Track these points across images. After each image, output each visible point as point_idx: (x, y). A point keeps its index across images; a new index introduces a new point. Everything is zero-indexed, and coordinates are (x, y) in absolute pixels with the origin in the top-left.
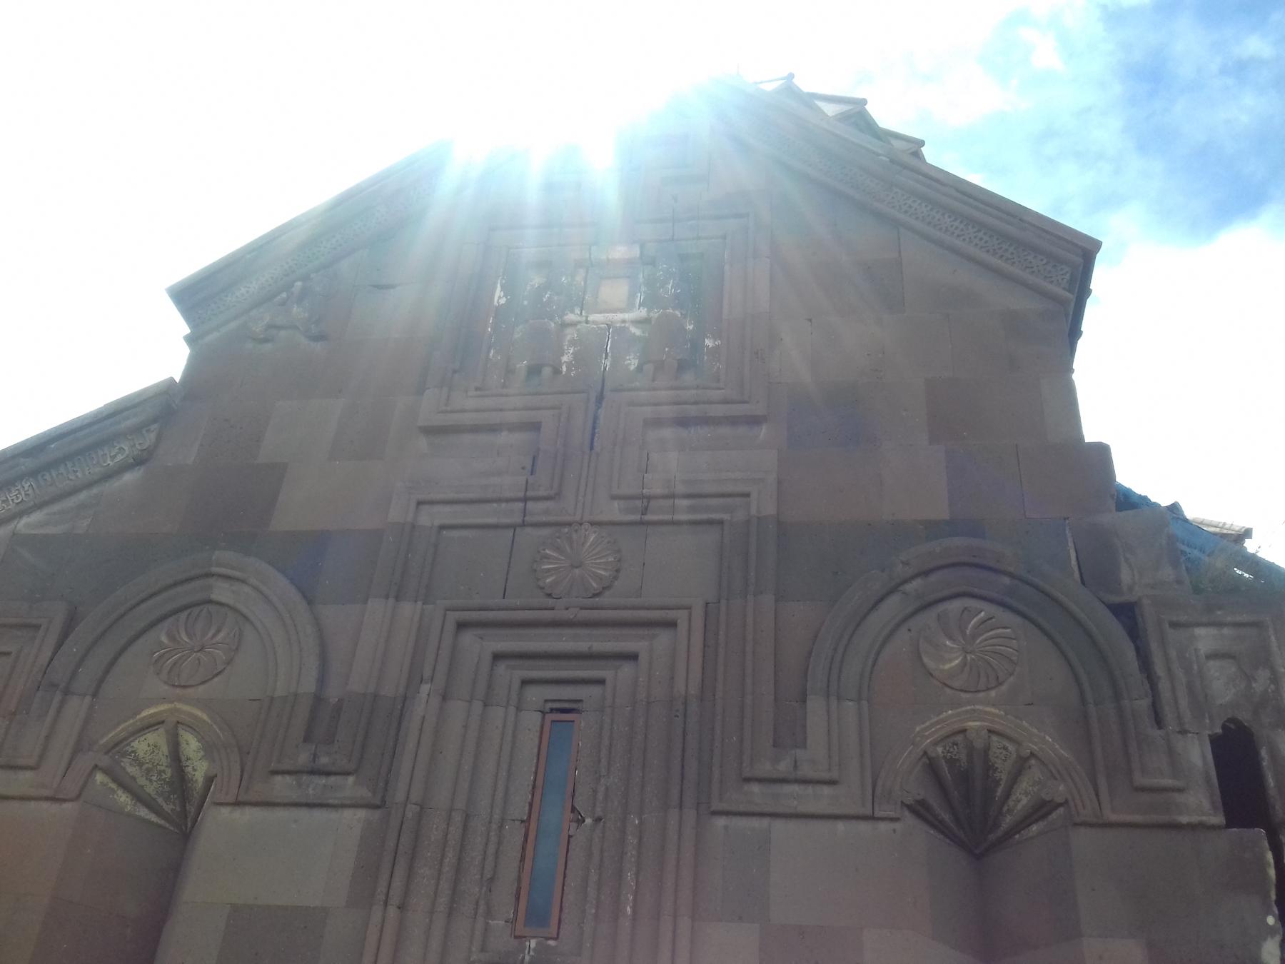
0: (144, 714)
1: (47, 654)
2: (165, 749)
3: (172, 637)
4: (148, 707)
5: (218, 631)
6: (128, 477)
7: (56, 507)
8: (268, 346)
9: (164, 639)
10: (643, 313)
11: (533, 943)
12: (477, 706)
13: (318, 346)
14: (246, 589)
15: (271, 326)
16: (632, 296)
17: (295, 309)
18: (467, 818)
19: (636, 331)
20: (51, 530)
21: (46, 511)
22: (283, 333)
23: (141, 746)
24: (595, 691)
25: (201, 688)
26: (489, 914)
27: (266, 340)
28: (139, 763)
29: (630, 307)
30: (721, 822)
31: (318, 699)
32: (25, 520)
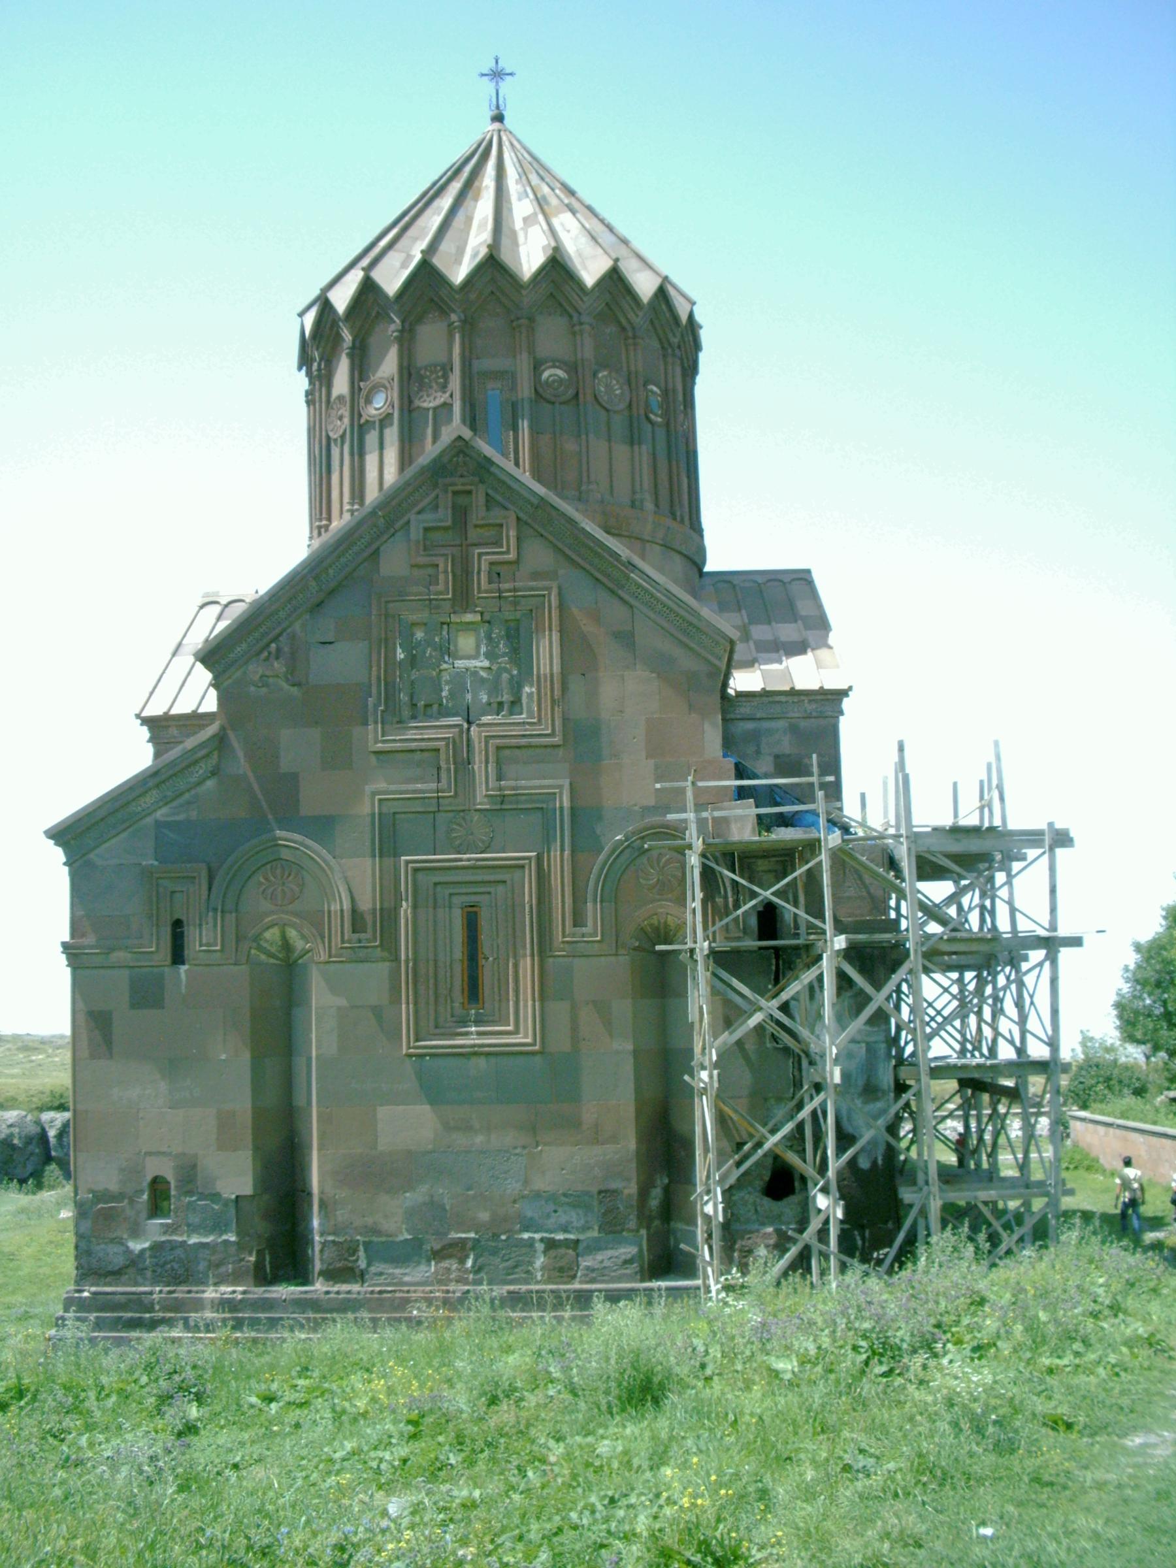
1: (205, 892)
3: (266, 879)
6: (210, 783)
9: (262, 880)
10: (486, 664)
11: (473, 1011)
12: (431, 910)
16: (478, 647)
17: (276, 664)
18: (436, 961)
19: (483, 674)
20: (177, 818)
23: (267, 935)
24: (487, 897)
26: (452, 1002)
28: (267, 941)
29: (476, 657)
30: (551, 960)
31: (354, 911)
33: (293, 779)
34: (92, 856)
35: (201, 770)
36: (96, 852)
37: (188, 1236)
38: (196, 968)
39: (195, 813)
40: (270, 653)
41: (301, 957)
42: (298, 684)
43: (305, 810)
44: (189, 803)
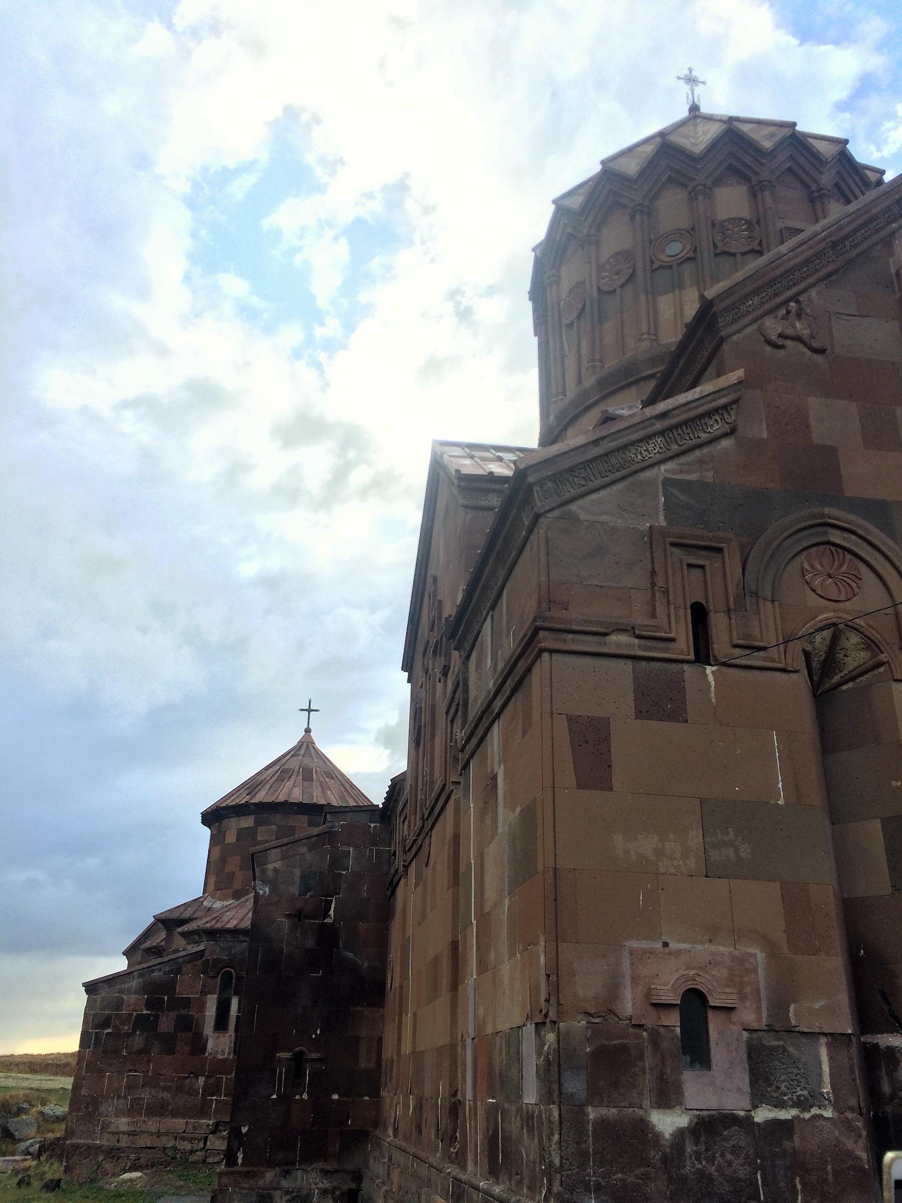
0: (820, 617)
2: (828, 642)
3: (812, 567)
4: (822, 613)
5: (841, 566)
6: (725, 443)
7: (683, 460)
8: (781, 353)
13: (819, 358)
14: (853, 537)
15: (781, 336)
17: (798, 325)
21: (675, 461)
22: (789, 343)
23: (818, 638)
25: (847, 603)
27: (782, 347)
32: (663, 467)
33: (830, 453)
34: (573, 507)
35: (716, 427)
36: (580, 502)
37: (755, 1107)
38: (725, 670)
39: (710, 474)
40: (788, 312)
41: (853, 679)
42: (821, 351)
43: (850, 491)
44: (701, 461)
